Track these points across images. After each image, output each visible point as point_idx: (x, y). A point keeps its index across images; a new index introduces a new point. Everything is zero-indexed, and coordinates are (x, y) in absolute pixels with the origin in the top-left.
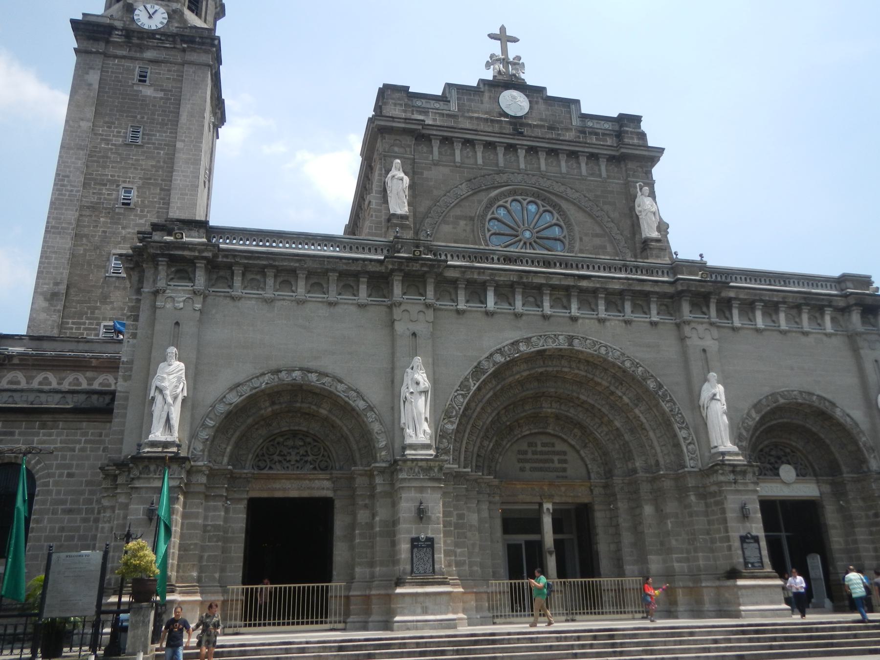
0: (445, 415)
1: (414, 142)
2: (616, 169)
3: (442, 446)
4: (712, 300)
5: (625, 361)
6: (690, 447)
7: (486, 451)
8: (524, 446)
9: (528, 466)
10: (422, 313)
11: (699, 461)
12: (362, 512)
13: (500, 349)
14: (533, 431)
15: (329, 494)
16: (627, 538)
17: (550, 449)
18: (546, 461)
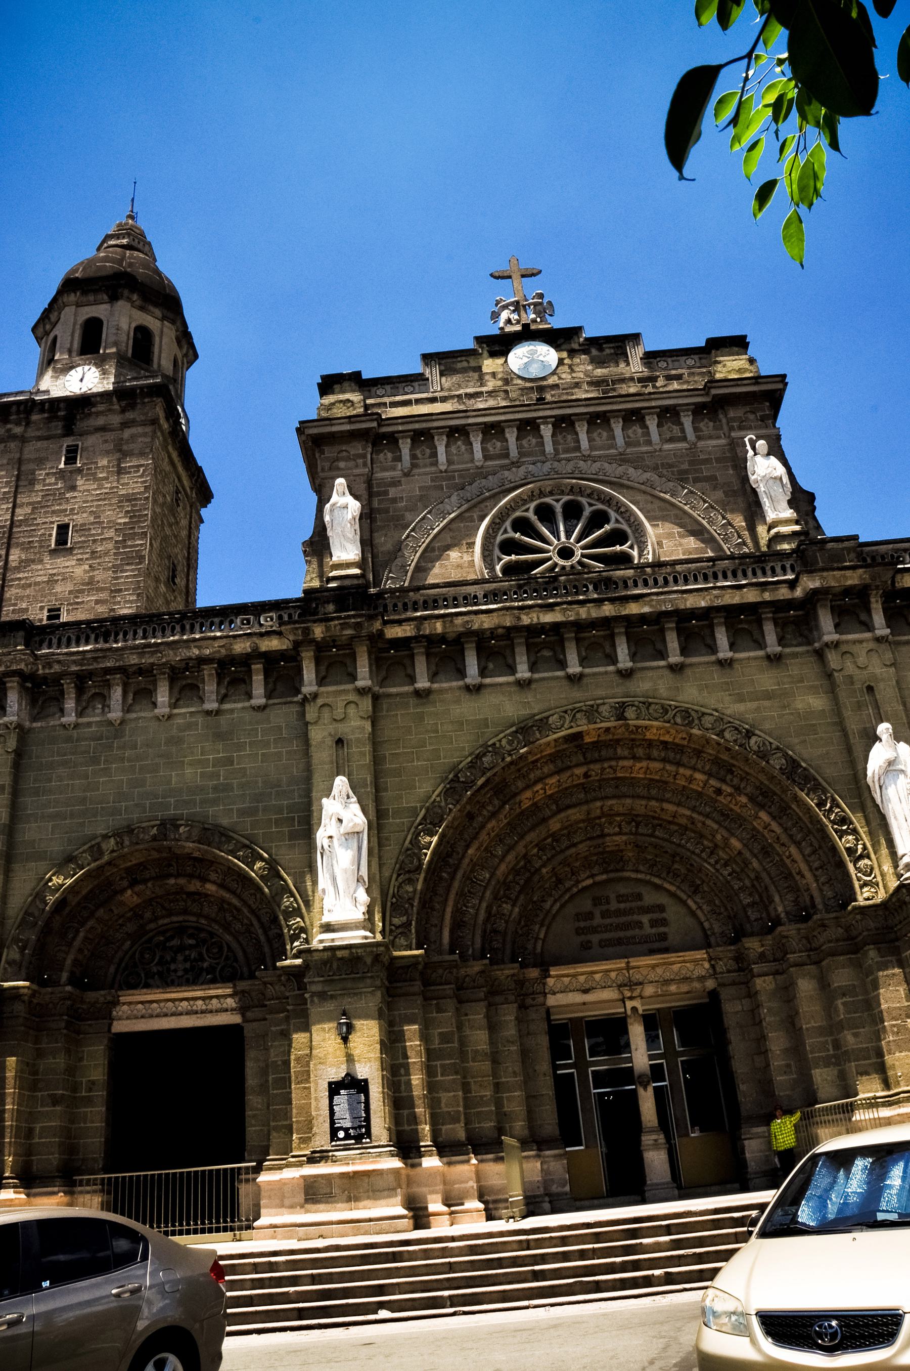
0: (400, 868)
1: (370, 449)
2: (711, 424)
3: (396, 921)
4: (873, 600)
5: (723, 731)
6: (861, 863)
7: (507, 922)
8: (586, 904)
9: (595, 938)
10: (353, 706)
11: (881, 885)
12: (276, 1043)
13: (494, 744)
14: (599, 878)
15: (236, 1019)
16: (777, 1042)
17: (634, 904)
18: (627, 926)
